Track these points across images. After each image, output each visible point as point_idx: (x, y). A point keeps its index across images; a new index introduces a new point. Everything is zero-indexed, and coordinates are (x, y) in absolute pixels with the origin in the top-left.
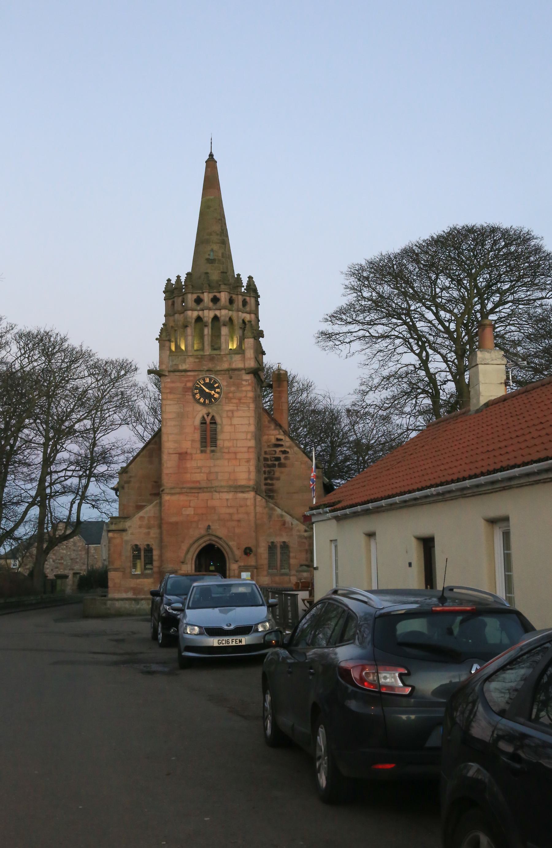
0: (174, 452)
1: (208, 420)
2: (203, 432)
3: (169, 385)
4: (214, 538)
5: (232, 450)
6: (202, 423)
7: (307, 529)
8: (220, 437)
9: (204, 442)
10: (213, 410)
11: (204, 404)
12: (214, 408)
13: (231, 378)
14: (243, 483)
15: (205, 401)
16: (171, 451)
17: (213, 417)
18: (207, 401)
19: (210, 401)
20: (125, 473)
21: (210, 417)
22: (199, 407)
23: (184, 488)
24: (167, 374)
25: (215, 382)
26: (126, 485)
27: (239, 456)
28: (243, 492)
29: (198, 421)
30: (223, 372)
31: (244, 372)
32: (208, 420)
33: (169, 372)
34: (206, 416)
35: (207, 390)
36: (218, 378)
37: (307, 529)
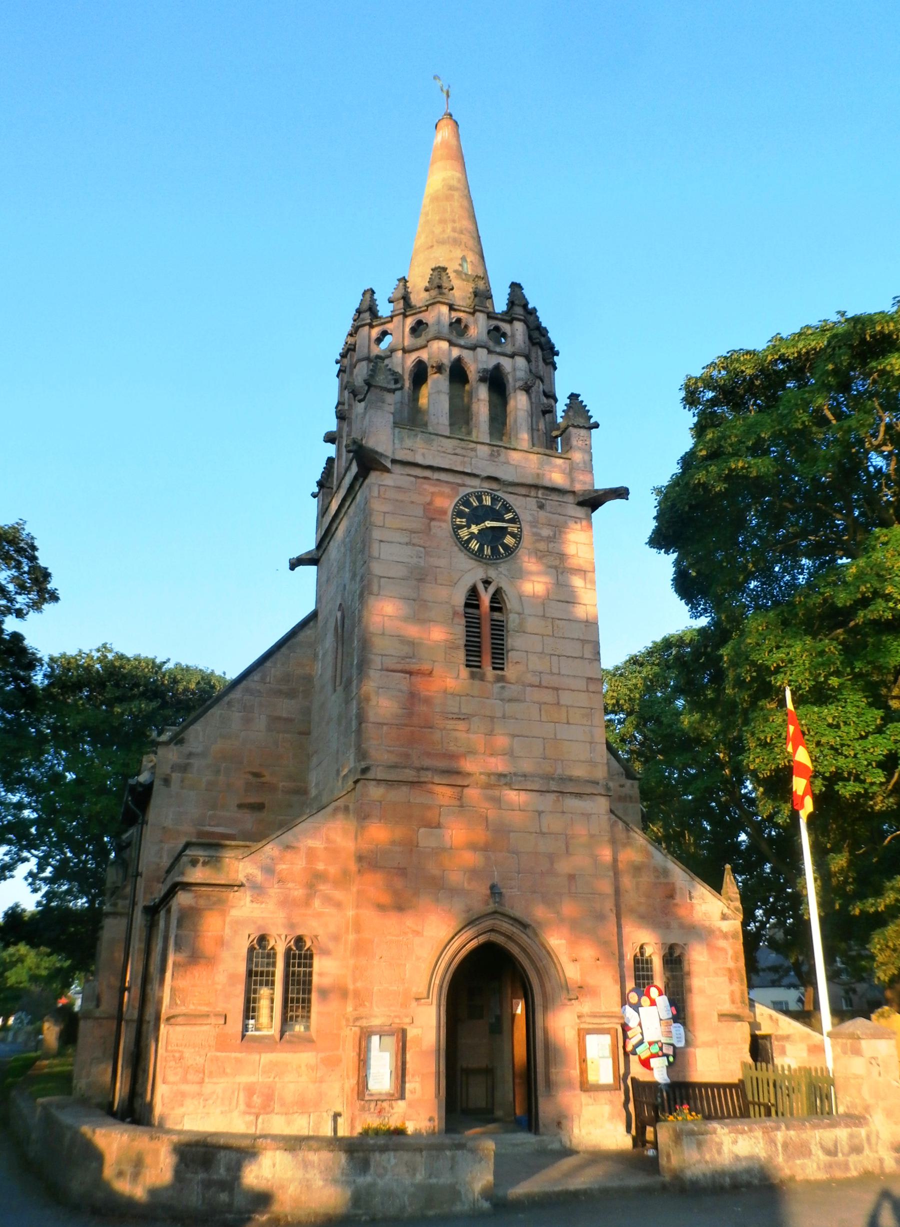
0: (399, 667)
1: (486, 599)
2: (473, 626)
3: (391, 494)
4: (506, 926)
5: (547, 680)
6: (467, 605)
7: (726, 910)
8: (513, 641)
9: (473, 651)
10: (499, 575)
11: (478, 555)
12: (503, 568)
13: (541, 507)
14: (579, 772)
15: (481, 549)
16: (390, 663)
17: (498, 593)
18: (487, 551)
19: (495, 551)
20: (176, 744)
21: (492, 589)
22: (463, 561)
23: (427, 769)
24: (389, 465)
25: (507, 508)
26: (175, 777)
27: (566, 698)
28: (579, 795)
29: (460, 598)
30: (523, 491)
31: (570, 499)
32: (486, 599)
33: (394, 461)
34: (481, 587)
35: (489, 524)
36: (511, 499)
37: (726, 910)
